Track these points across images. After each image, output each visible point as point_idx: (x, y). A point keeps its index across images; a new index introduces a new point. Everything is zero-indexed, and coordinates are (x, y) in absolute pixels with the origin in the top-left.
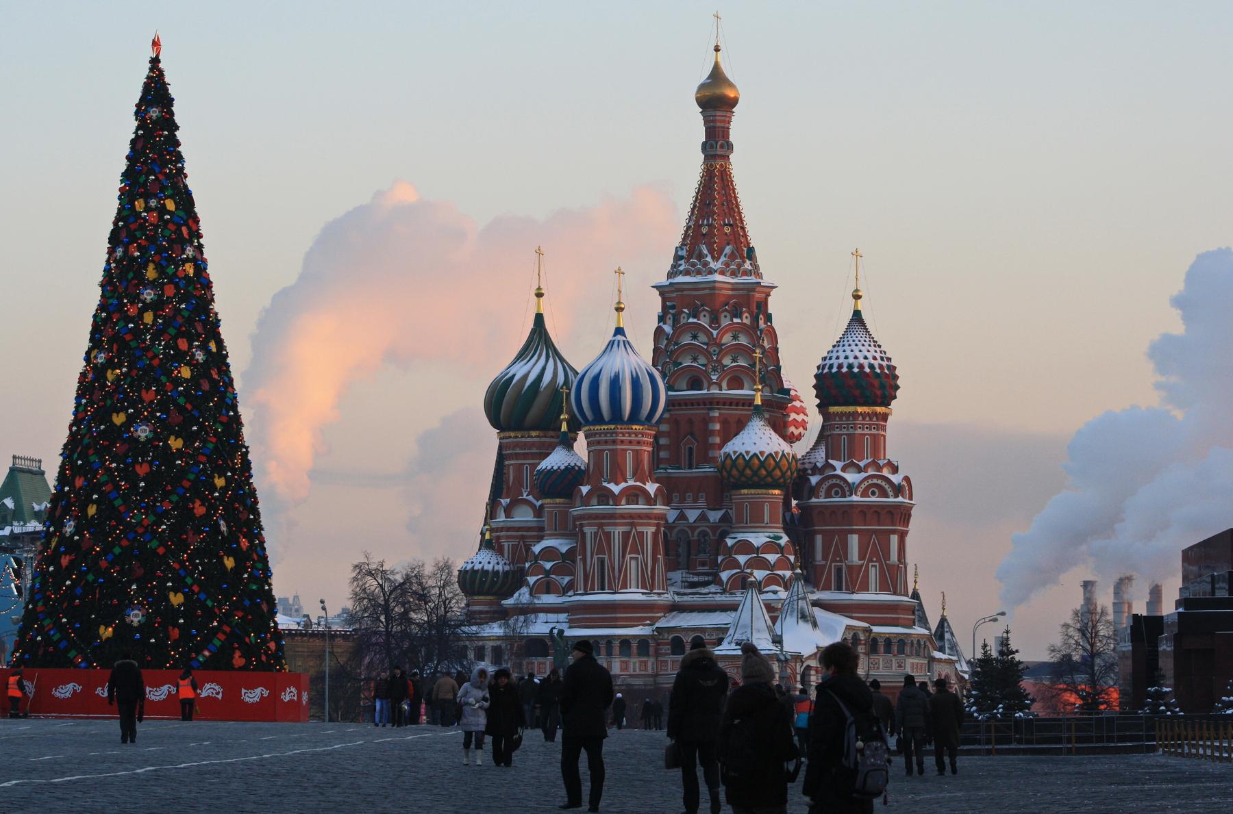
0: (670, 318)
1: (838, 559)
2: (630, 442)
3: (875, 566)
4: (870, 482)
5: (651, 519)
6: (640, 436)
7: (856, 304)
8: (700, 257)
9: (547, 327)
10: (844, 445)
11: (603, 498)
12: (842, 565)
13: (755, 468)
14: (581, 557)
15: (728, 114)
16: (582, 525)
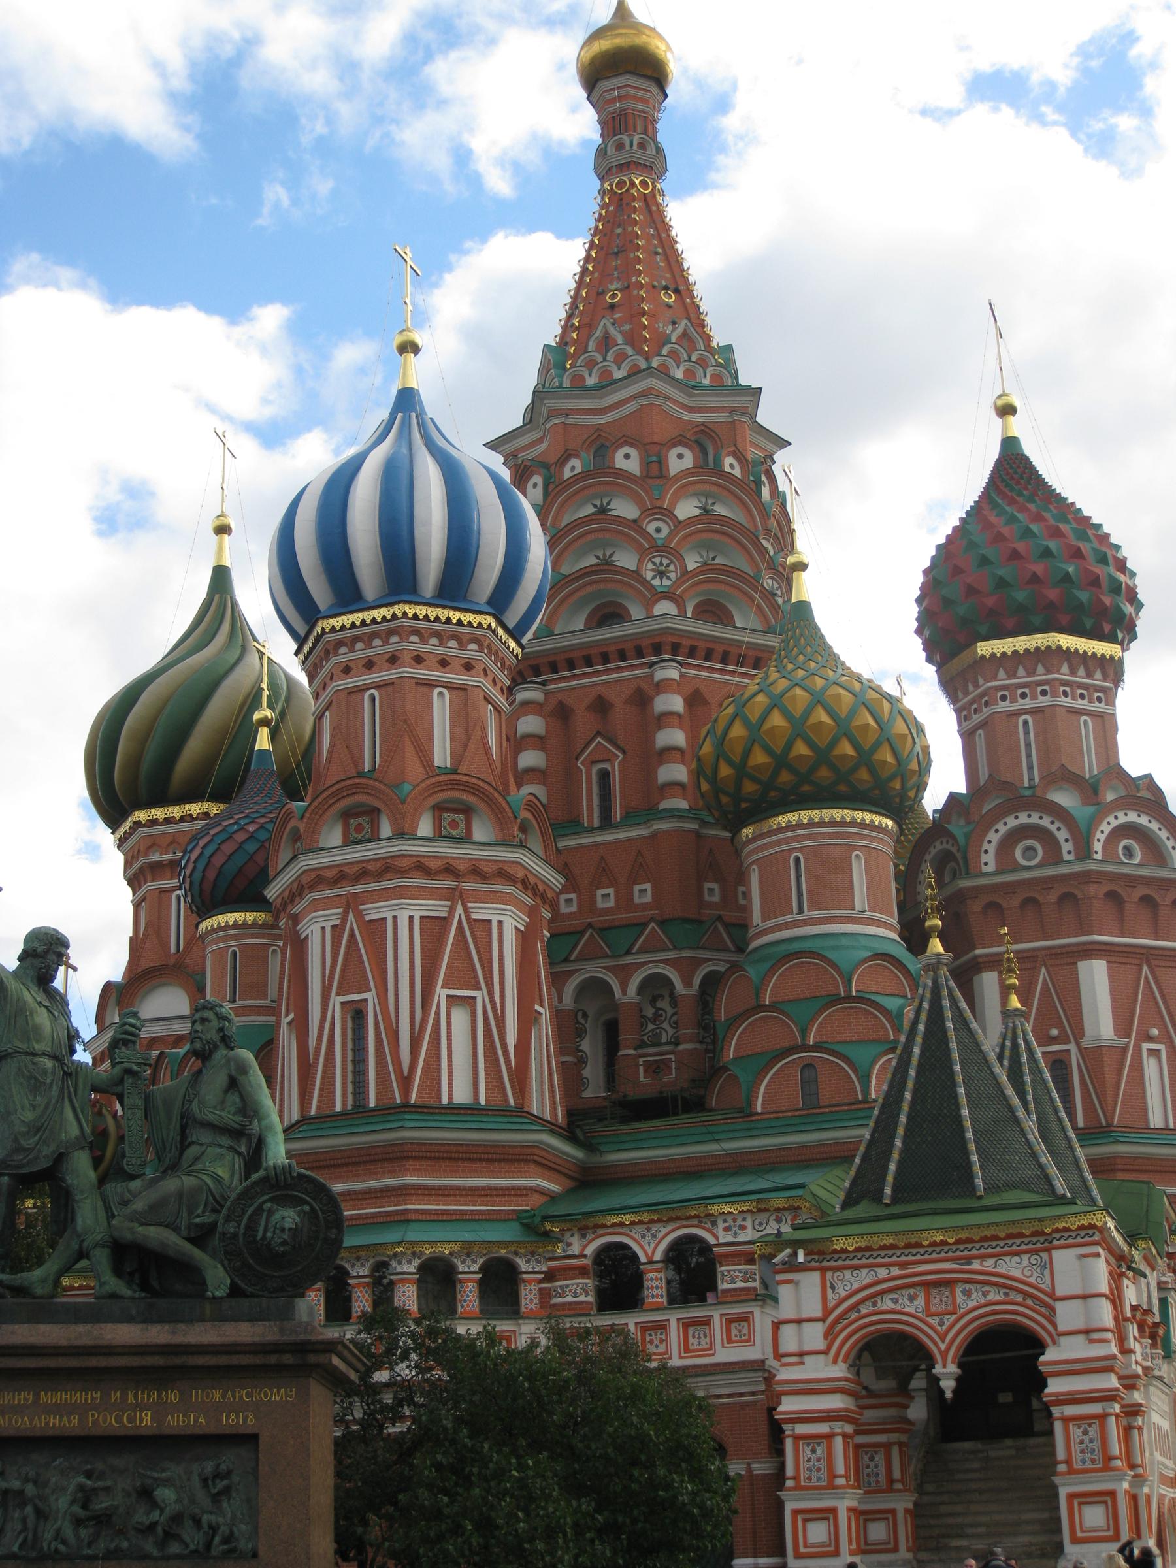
0: (535, 485)
1: (1054, 1032)
2: (444, 663)
3: (1159, 1050)
4: (1123, 818)
5: (510, 879)
6: (473, 646)
7: (1005, 428)
8: (607, 345)
9: (238, 598)
10: (1028, 745)
11: (360, 820)
12: (1068, 1051)
13: (822, 743)
14: (292, 1016)
15: (655, 90)
16: (296, 919)
